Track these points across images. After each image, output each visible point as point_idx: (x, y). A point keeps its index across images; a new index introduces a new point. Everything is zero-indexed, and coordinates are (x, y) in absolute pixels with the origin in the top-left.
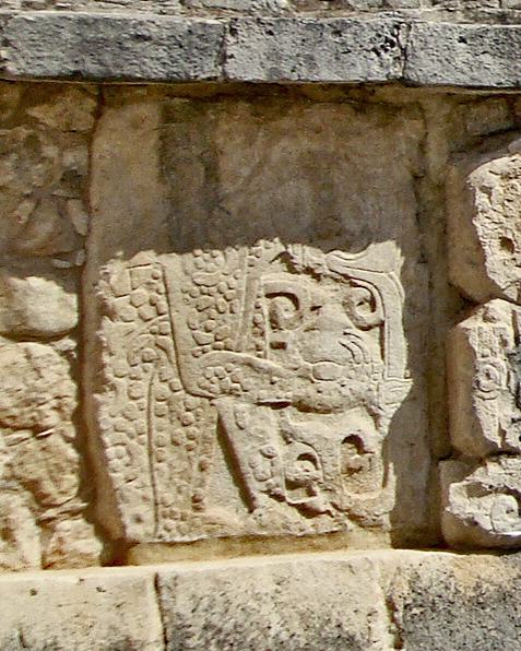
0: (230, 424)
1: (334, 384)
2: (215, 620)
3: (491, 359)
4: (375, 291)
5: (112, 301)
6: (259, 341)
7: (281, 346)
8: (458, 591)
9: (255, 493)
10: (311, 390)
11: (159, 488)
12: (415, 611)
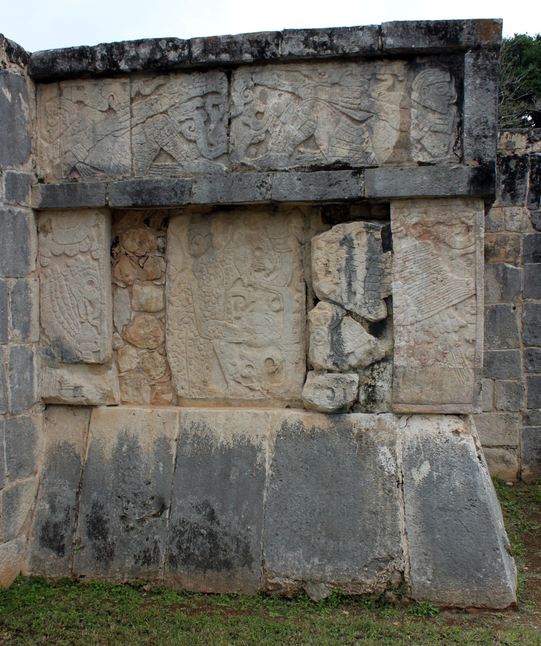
0: (218, 351)
1: (261, 336)
2: (199, 433)
3: (320, 327)
4: (280, 295)
5: (172, 298)
6: (230, 316)
7: (239, 318)
8: (303, 431)
9: (228, 380)
10: (251, 337)
11: (190, 376)
12: (282, 438)
